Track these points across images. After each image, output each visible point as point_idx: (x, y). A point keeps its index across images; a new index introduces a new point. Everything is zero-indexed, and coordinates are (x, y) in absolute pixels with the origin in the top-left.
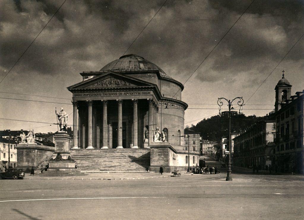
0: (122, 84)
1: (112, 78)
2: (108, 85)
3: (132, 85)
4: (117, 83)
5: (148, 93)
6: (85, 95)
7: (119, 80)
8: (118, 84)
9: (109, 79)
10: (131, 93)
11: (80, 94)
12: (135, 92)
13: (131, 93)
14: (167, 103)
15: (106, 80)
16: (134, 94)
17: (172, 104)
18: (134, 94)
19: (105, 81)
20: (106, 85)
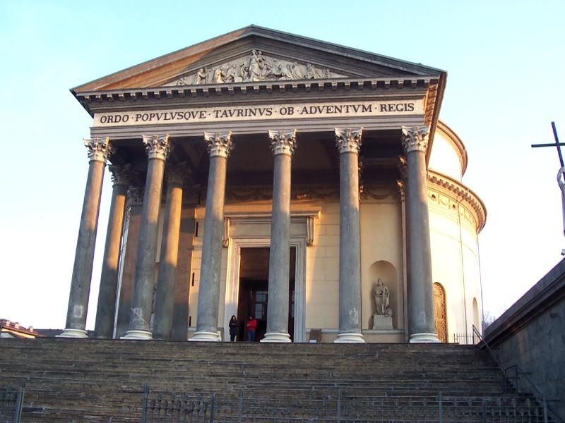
0: (293, 72)
1: (255, 56)
4: (275, 71)
5: (403, 107)
6: (140, 120)
7: (283, 64)
8: (281, 76)
9: (244, 61)
10: (333, 109)
12: (347, 104)
13: (333, 109)
14: (436, 195)
15: (232, 63)
16: (344, 110)
17: (452, 203)
18: (344, 110)
19: (225, 66)
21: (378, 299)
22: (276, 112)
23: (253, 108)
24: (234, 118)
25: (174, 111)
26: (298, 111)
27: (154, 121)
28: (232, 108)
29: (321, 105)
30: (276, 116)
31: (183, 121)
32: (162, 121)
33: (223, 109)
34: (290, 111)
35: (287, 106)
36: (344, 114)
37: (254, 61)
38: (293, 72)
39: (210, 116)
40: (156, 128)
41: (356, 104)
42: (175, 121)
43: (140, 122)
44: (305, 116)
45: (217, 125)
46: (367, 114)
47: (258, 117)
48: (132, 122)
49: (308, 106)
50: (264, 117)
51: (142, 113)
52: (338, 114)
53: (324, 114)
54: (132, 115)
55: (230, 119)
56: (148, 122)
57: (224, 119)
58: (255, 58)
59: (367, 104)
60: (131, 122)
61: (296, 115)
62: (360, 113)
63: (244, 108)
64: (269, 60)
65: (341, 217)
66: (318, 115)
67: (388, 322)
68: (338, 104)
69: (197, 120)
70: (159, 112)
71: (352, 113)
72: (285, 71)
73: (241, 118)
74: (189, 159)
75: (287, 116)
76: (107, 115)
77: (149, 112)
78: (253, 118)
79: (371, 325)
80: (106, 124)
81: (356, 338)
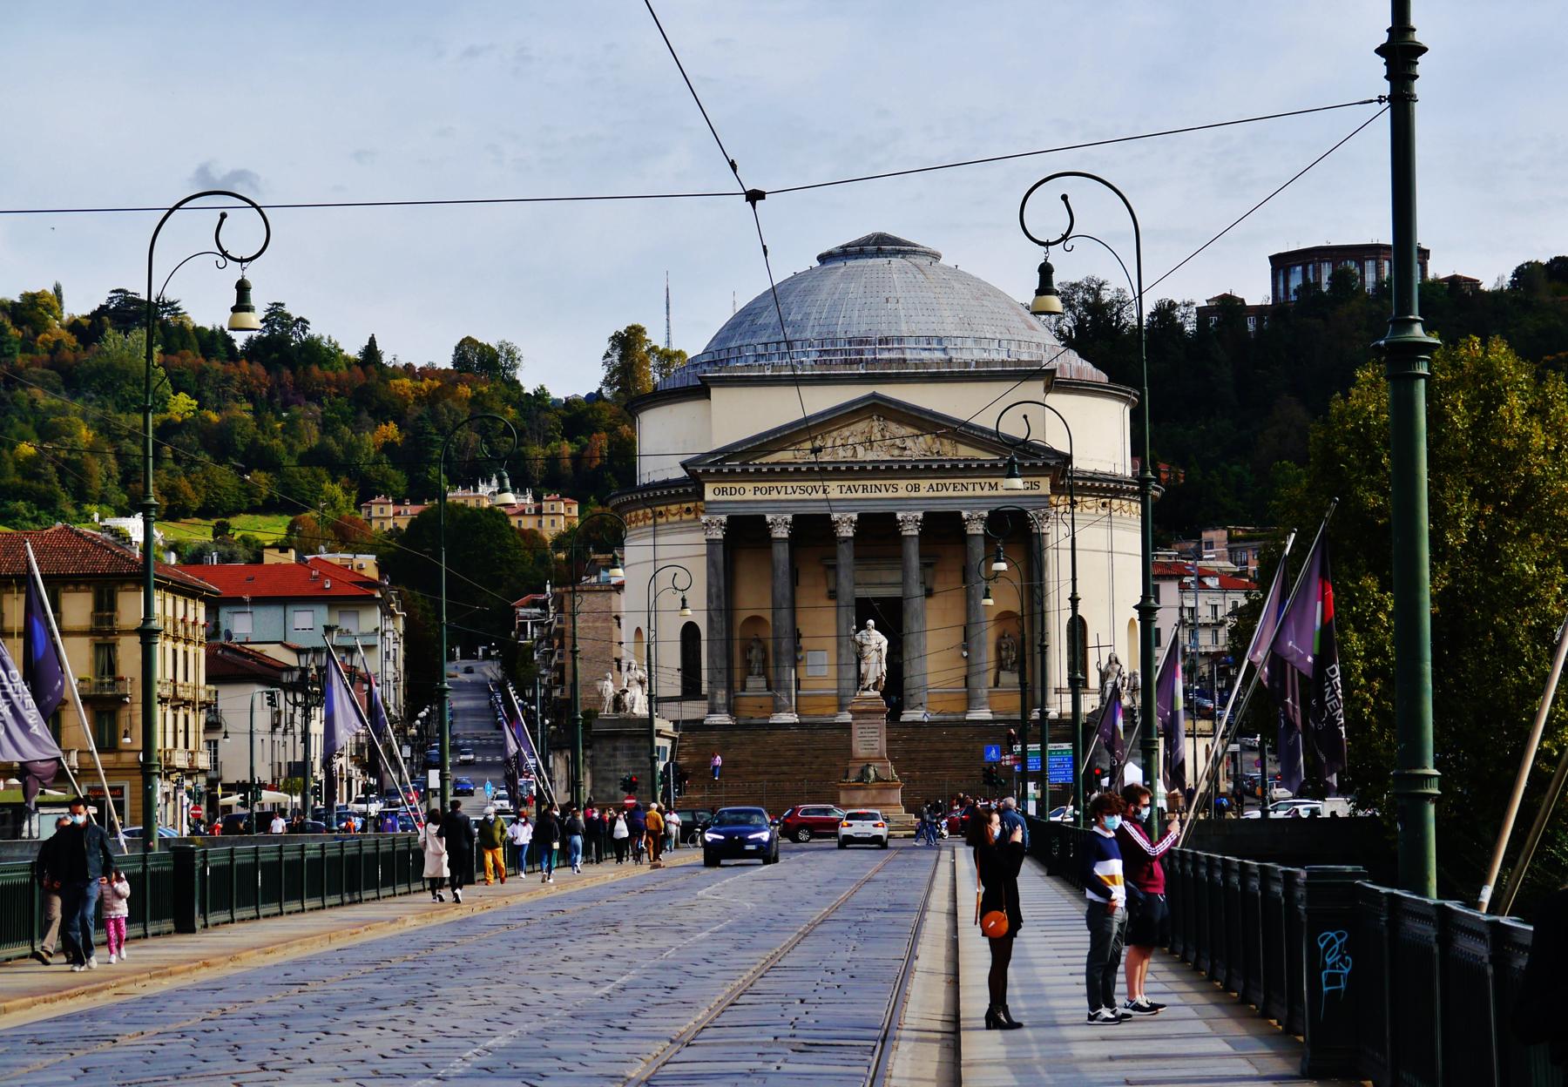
0: (918, 447)
2: (860, 450)
3: (965, 452)
9: (862, 426)
11: (738, 486)
15: (852, 428)
20: (850, 453)
21: (1004, 653)
22: (902, 488)
23: (878, 483)
24: (860, 495)
25: (795, 484)
26: (925, 488)
27: (774, 495)
28: (857, 483)
29: (947, 481)
30: (902, 493)
31: (806, 496)
32: (782, 496)
33: (847, 483)
34: (917, 488)
35: (913, 482)
36: (970, 493)
37: (875, 430)
38: (918, 447)
39: (835, 490)
40: (778, 502)
41: (982, 481)
42: (797, 496)
43: (759, 496)
44: (931, 494)
45: (843, 501)
46: (994, 493)
47: (884, 494)
48: (749, 496)
49: (934, 482)
50: (890, 494)
51: (760, 485)
52: (964, 493)
53: (951, 493)
54: (749, 486)
55: (854, 495)
56: (767, 497)
57: (849, 495)
58: (876, 426)
59: (993, 481)
60: (748, 494)
61: (923, 493)
62: (986, 492)
63: (868, 483)
64: (893, 427)
65: (968, 601)
66: (944, 493)
67: (1015, 678)
68: (964, 481)
69: (821, 495)
70: (779, 484)
71: (978, 492)
72: (909, 443)
73: (866, 495)
74: (813, 530)
75: (913, 494)
76: (721, 485)
77: (767, 485)
78: (879, 495)
79: (996, 685)
80: (720, 498)
81: (984, 714)
